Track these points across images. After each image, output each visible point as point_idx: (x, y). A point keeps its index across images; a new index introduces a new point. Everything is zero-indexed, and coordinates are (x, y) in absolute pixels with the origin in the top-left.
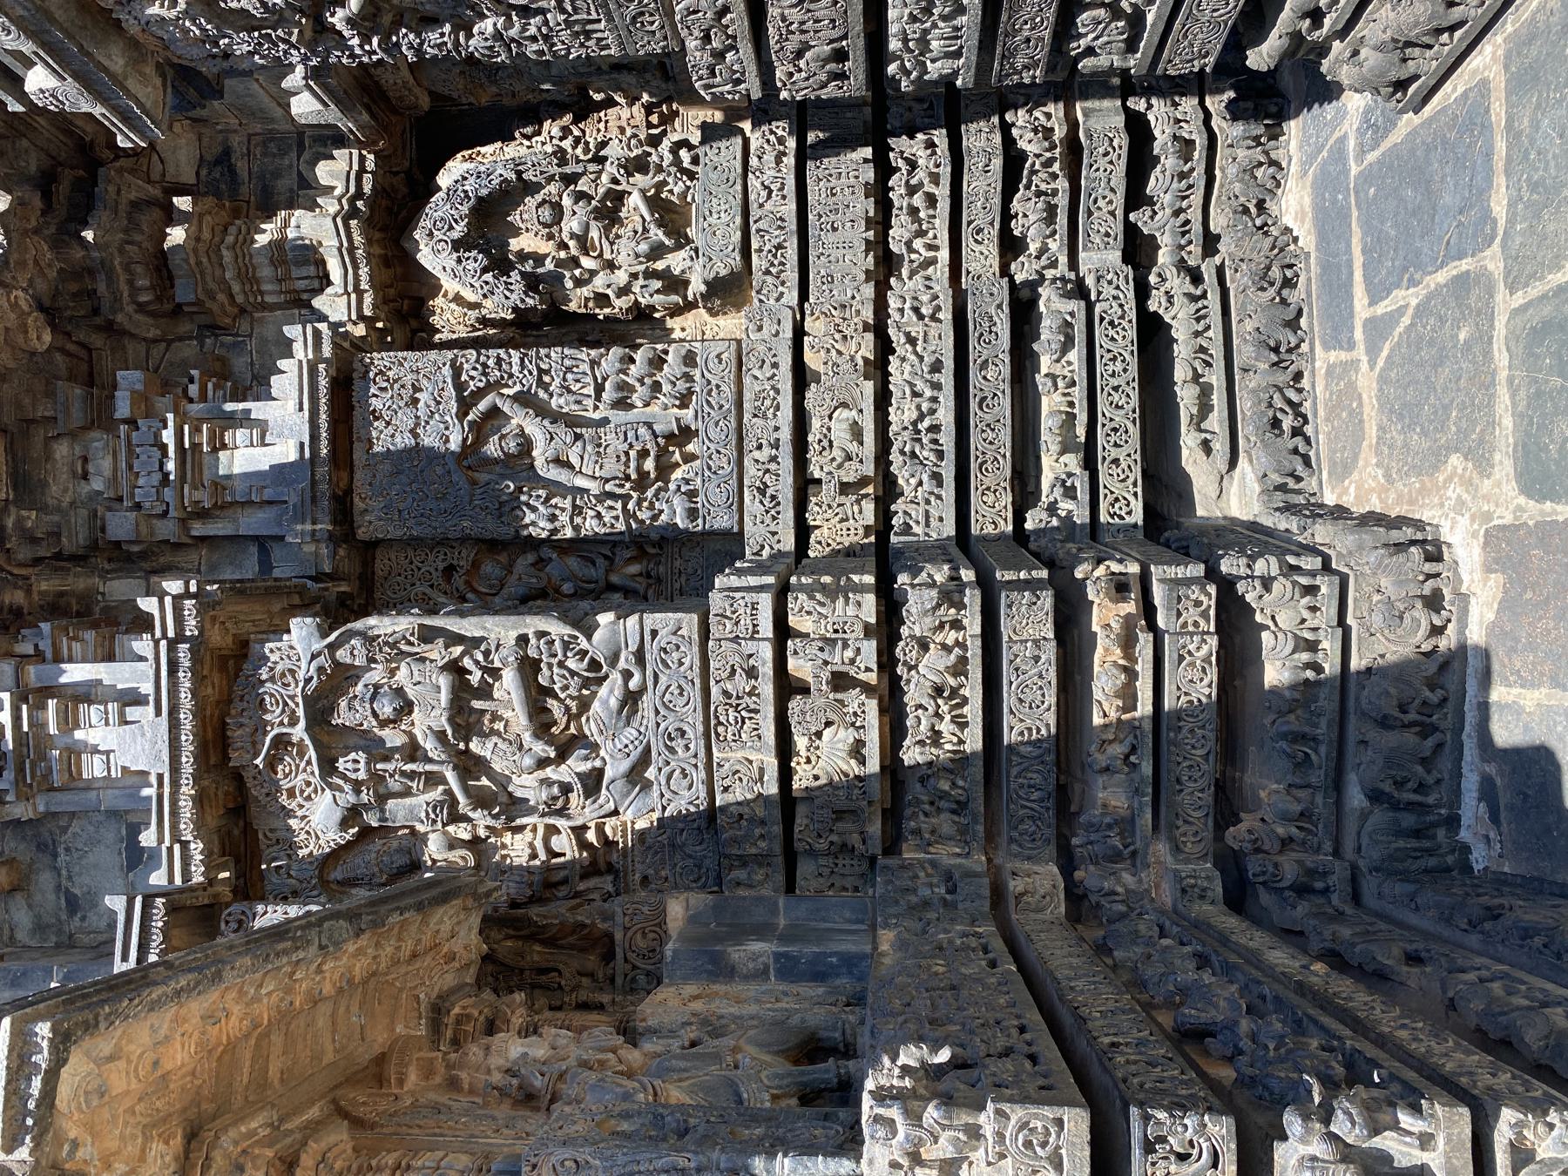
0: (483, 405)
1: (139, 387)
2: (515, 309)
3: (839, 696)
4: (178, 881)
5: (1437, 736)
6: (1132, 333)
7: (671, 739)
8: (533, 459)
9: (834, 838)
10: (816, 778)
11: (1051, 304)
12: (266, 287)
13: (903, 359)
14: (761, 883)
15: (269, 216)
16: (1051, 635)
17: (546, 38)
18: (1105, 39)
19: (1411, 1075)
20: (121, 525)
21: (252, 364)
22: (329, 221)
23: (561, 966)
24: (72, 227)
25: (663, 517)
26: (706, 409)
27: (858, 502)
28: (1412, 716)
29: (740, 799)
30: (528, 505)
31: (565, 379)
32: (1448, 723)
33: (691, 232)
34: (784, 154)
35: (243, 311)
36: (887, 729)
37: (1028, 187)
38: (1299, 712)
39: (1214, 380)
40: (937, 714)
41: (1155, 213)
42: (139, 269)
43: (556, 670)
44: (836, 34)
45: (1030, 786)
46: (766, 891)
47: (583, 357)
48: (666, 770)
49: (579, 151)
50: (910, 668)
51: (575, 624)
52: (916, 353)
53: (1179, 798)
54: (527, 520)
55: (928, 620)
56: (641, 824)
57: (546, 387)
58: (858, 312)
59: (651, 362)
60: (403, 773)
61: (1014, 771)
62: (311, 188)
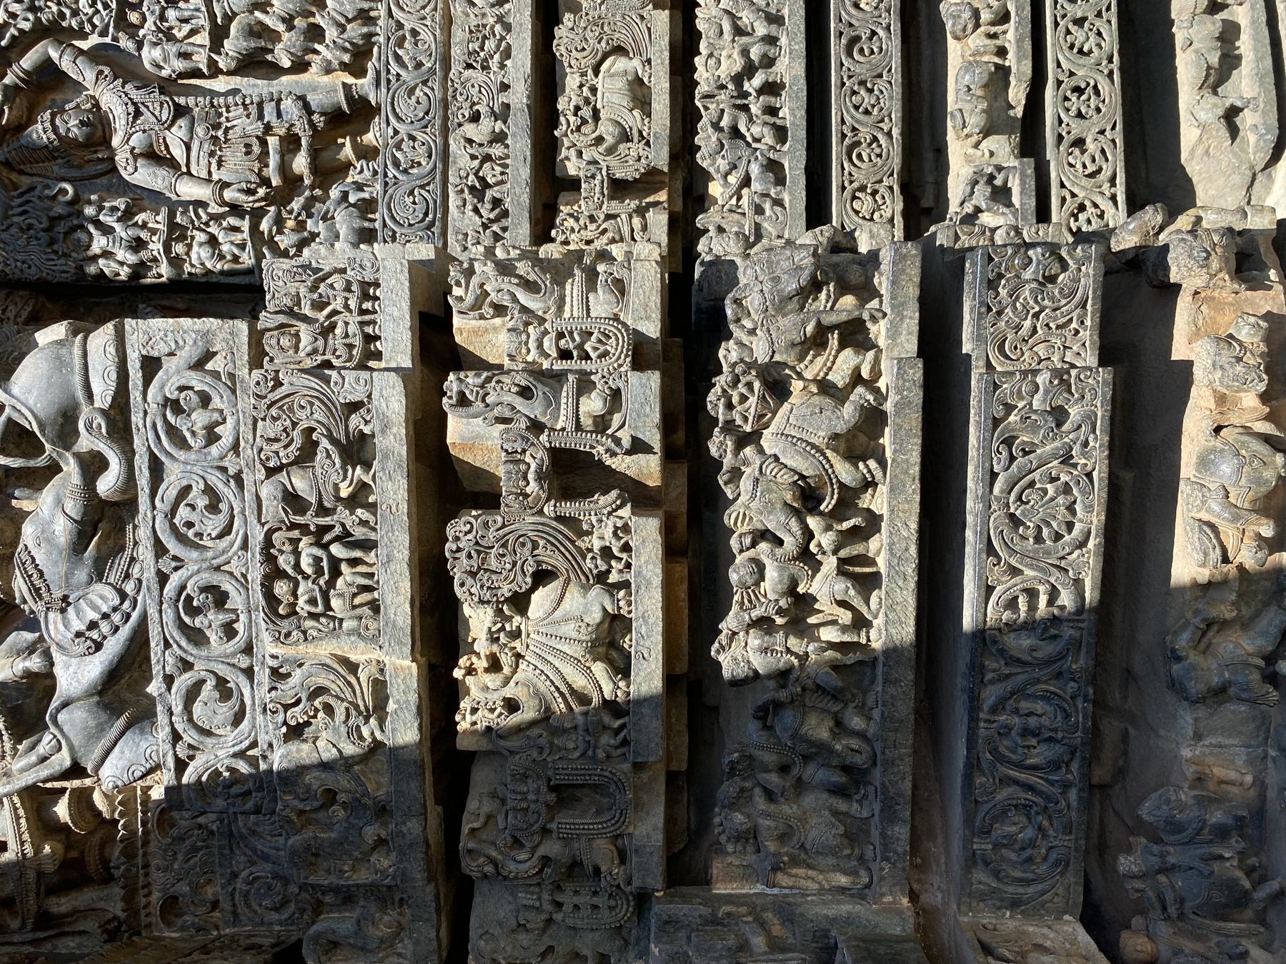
0: (28, 61)
3: (568, 508)
7: (194, 611)
9: (551, 848)
10: (512, 706)
26: (394, 68)
27: (641, 211)
29: (328, 754)
31: (162, 18)
36: (682, 591)
40: (806, 556)
45: (1026, 732)
48: (184, 681)
50: (744, 440)
54: (96, 249)
57: (132, 30)
61: (990, 695)
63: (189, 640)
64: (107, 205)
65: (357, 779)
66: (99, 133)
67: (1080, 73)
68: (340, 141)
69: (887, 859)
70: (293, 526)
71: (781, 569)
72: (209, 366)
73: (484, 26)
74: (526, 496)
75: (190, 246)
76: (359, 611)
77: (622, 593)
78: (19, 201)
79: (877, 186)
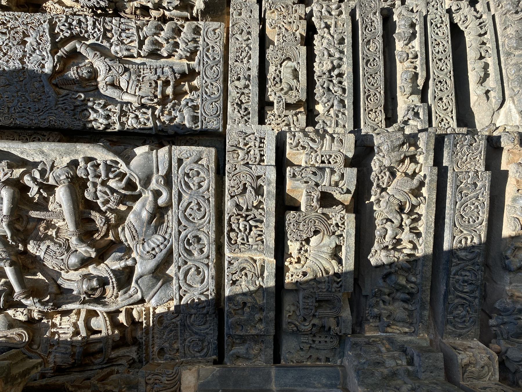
0: (67, 47)
3: (326, 210)
8: (98, 83)
9: (316, 321)
10: (305, 274)
14: (256, 356)
25: (177, 120)
26: (206, 59)
27: (296, 114)
29: (245, 290)
30: (93, 109)
31: (120, 36)
40: (401, 226)
43: (99, 188)
45: (464, 281)
46: (260, 362)
48: (184, 268)
50: (384, 190)
52: (330, 34)
54: (91, 118)
56: (160, 310)
57: (108, 39)
58: (296, 11)
59: (173, 30)
61: (454, 270)
63: (188, 254)
64: (96, 102)
65: (254, 298)
66: (93, 76)
67: (441, 77)
68: (182, 83)
69: (421, 322)
70: (238, 215)
71: (393, 230)
72: (200, 163)
73: (242, 47)
74: (313, 206)
75: (128, 119)
76: (257, 242)
77: (342, 238)
78: (61, 99)
79: (376, 110)
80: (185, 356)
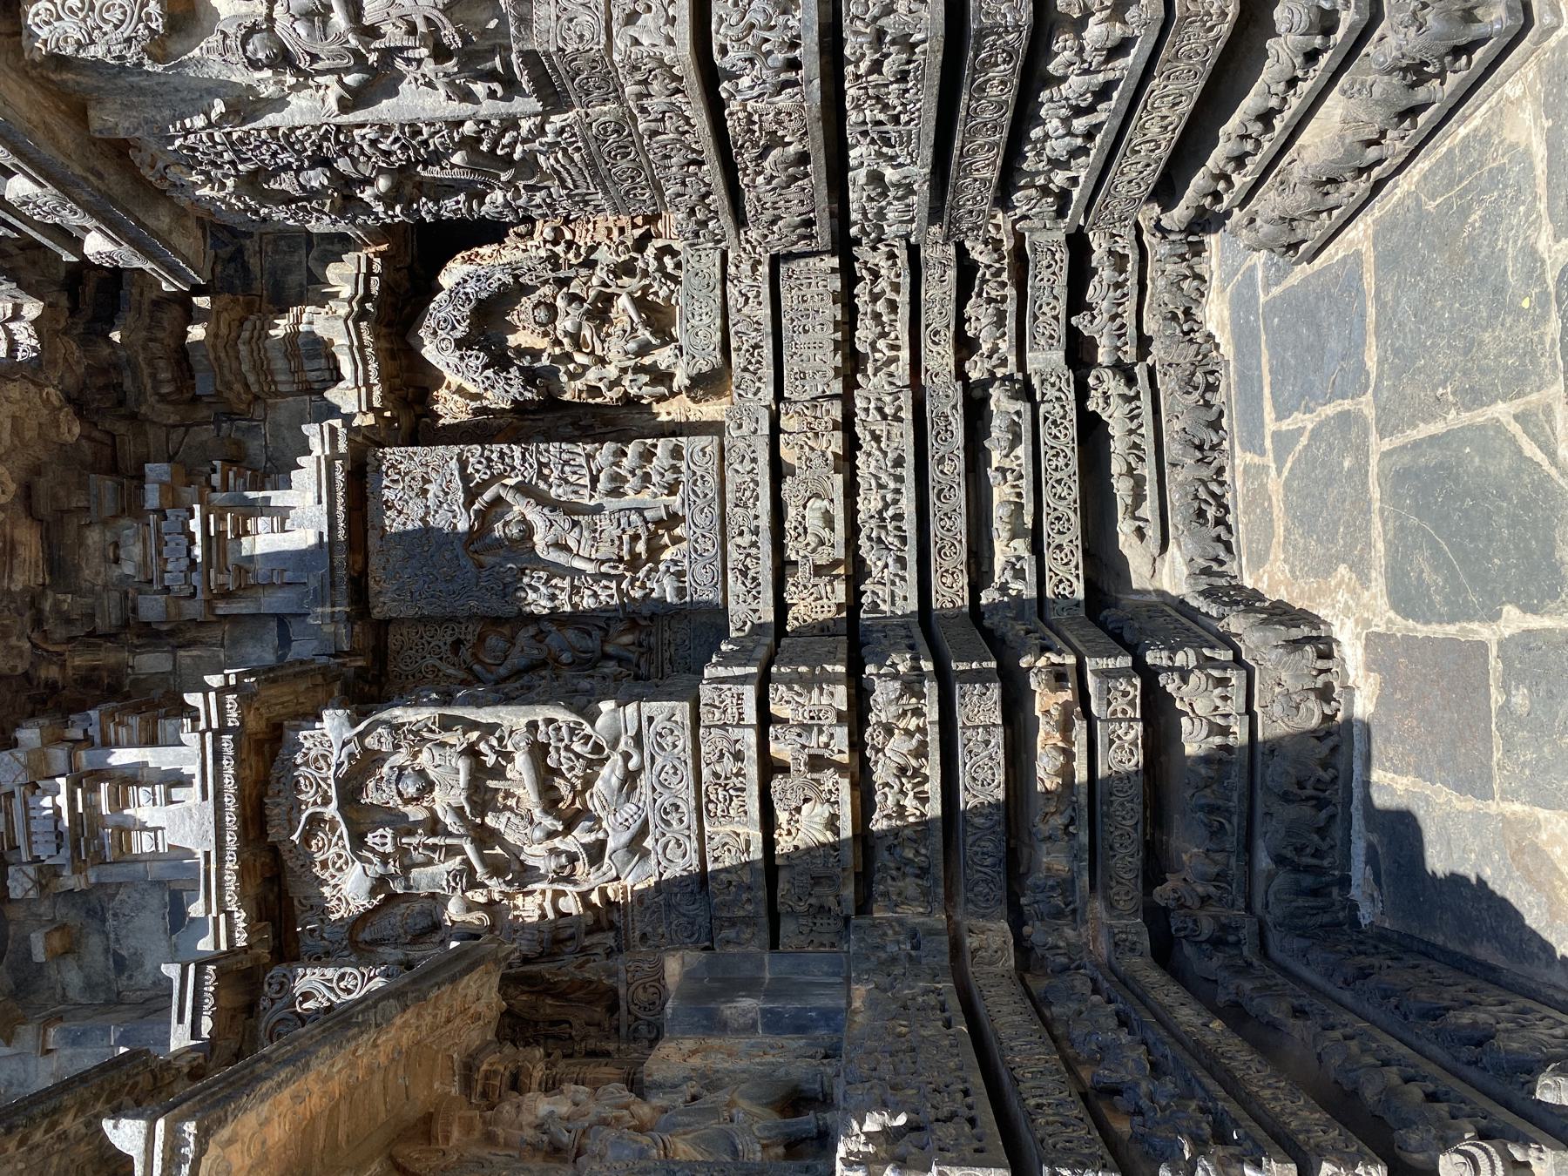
0: (488, 495)
1: (166, 478)
2: (515, 401)
3: (816, 776)
4: (224, 947)
5: (1330, 809)
6: (1073, 432)
7: (667, 813)
9: (812, 901)
11: (1000, 402)
12: (279, 378)
13: (869, 455)
14: (748, 941)
15: (283, 311)
16: (999, 722)
17: (549, 206)
18: (1037, 210)
19: (1260, 1134)
20: (151, 608)
21: (266, 446)
22: (341, 322)
23: (571, 1019)
24: (98, 326)
25: (654, 595)
26: (692, 497)
27: (831, 582)
28: (1309, 792)
30: (530, 586)
31: (563, 472)
32: (1338, 798)
33: (676, 331)
34: (759, 262)
35: (256, 398)
37: (979, 295)
38: (1215, 787)
39: (1146, 473)
40: (901, 791)
41: (1094, 317)
42: (162, 363)
43: (563, 753)
44: (804, 209)
46: (753, 948)
47: (579, 450)
48: (662, 841)
49: (571, 255)
50: (878, 750)
51: (580, 712)
52: (880, 449)
53: (1112, 862)
55: (893, 708)
57: (545, 479)
58: (828, 411)
59: (641, 455)
60: (426, 846)
61: (970, 840)
62: (319, 282)
80: (672, 942)
